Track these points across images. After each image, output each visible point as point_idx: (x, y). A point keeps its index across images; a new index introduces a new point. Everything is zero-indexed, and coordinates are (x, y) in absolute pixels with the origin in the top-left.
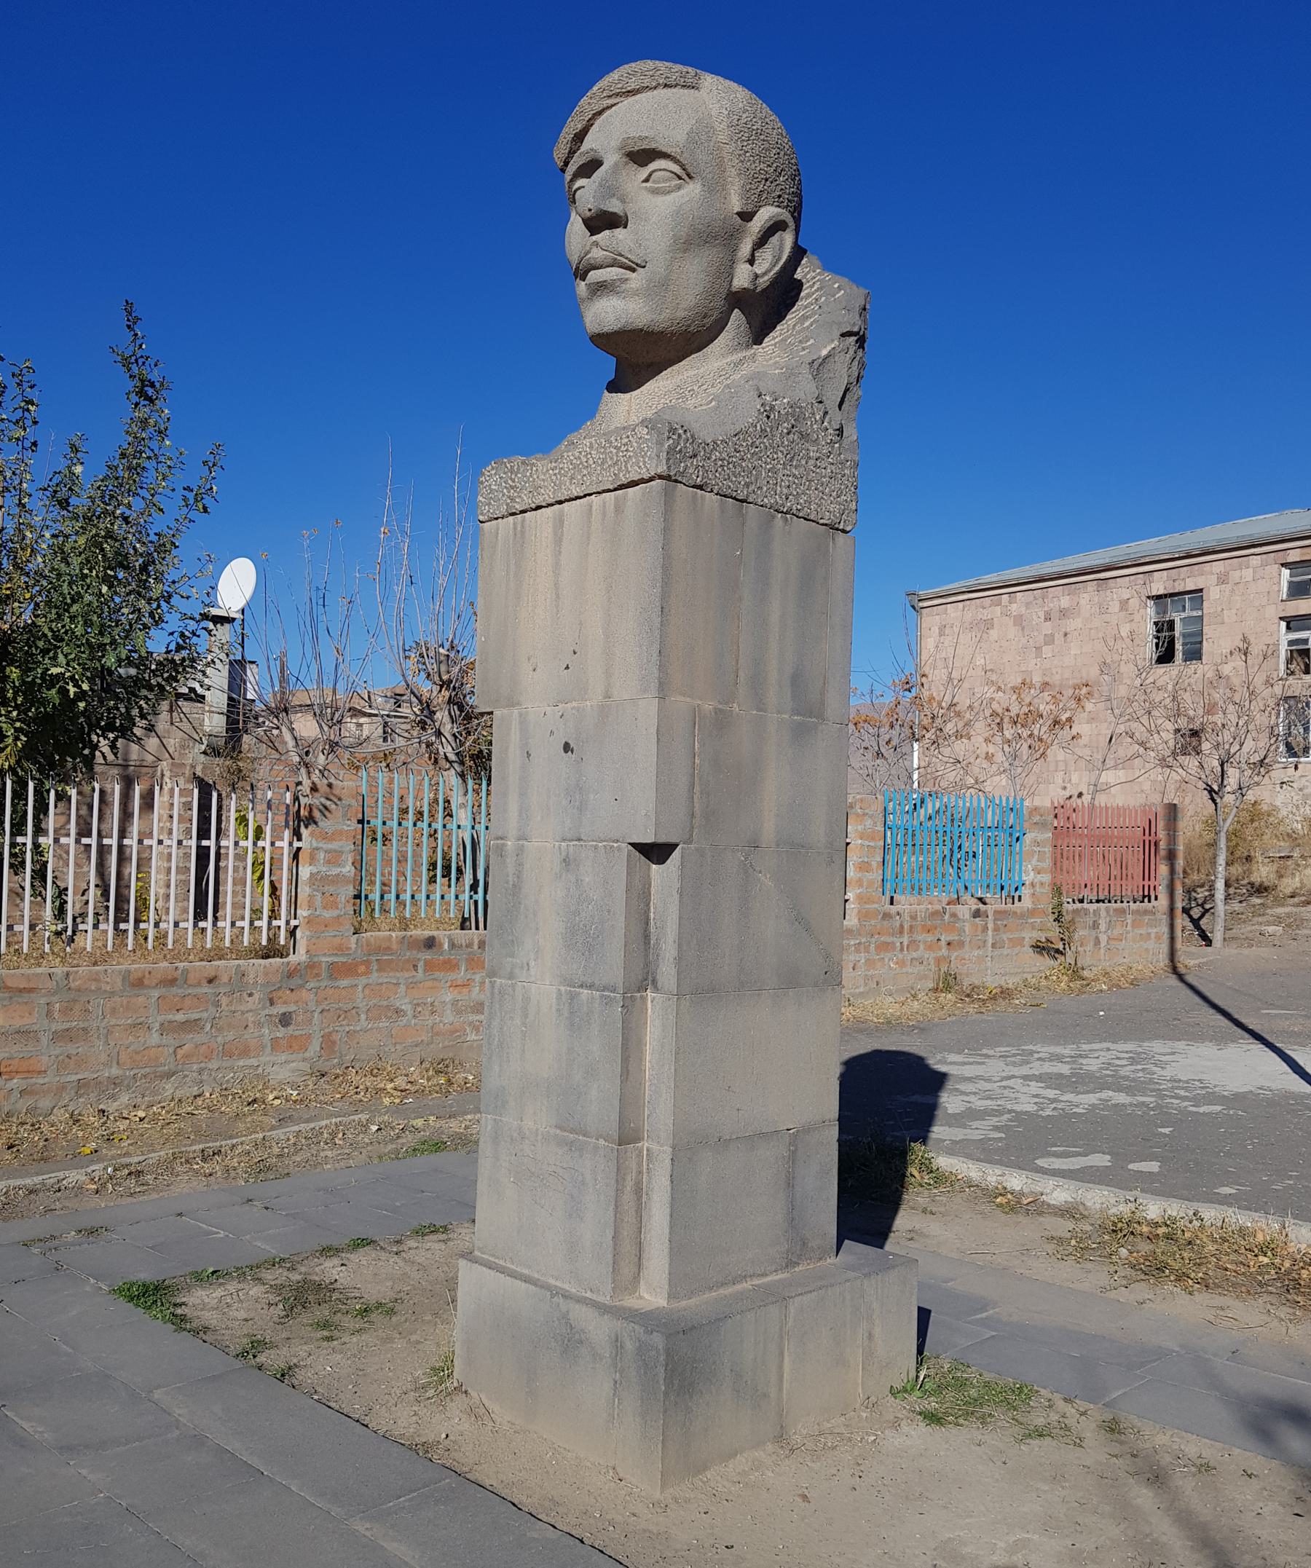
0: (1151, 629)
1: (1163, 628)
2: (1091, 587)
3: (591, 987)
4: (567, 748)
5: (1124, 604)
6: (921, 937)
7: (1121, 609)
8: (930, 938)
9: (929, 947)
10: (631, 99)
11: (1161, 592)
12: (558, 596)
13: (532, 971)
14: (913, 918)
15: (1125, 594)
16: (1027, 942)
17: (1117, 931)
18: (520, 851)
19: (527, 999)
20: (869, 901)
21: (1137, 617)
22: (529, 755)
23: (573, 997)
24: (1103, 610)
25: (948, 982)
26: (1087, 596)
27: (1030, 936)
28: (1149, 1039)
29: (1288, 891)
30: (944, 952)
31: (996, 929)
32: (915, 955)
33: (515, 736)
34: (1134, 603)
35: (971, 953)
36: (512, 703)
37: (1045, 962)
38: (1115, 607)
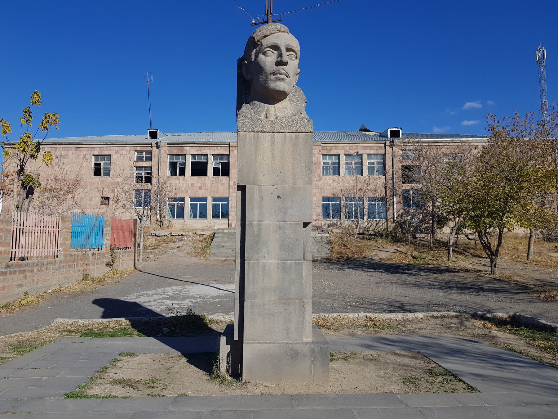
0: (93, 165)
1: (97, 165)
2: (73, 149)
3: (291, 260)
4: (278, 197)
5: (85, 156)
6: (79, 262)
7: (84, 158)
8: (82, 263)
9: (81, 266)
10: (281, 33)
11: (97, 154)
12: (273, 157)
13: (267, 258)
14: (78, 256)
15: (85, 153)
16: (105, 263)
17: (124, 258)
18: (259, 225)
19: (264, 267)
20: (67, 251)
21: (89, 161)
22: (262, 198)
23: (283, 264)
24: (77, 157)
25: (85, 278)
26: (71, 152)
27: (106, 260)
28: (166, 287)
29: (148, 245)
30: (85, 267)
31: (98, 259)
32: (78, 269)
33: (256, 193)
34: (88, 156)
35: (91, 267)
36: (254, 183)
37: (108, 269)
38: (81, 157)
